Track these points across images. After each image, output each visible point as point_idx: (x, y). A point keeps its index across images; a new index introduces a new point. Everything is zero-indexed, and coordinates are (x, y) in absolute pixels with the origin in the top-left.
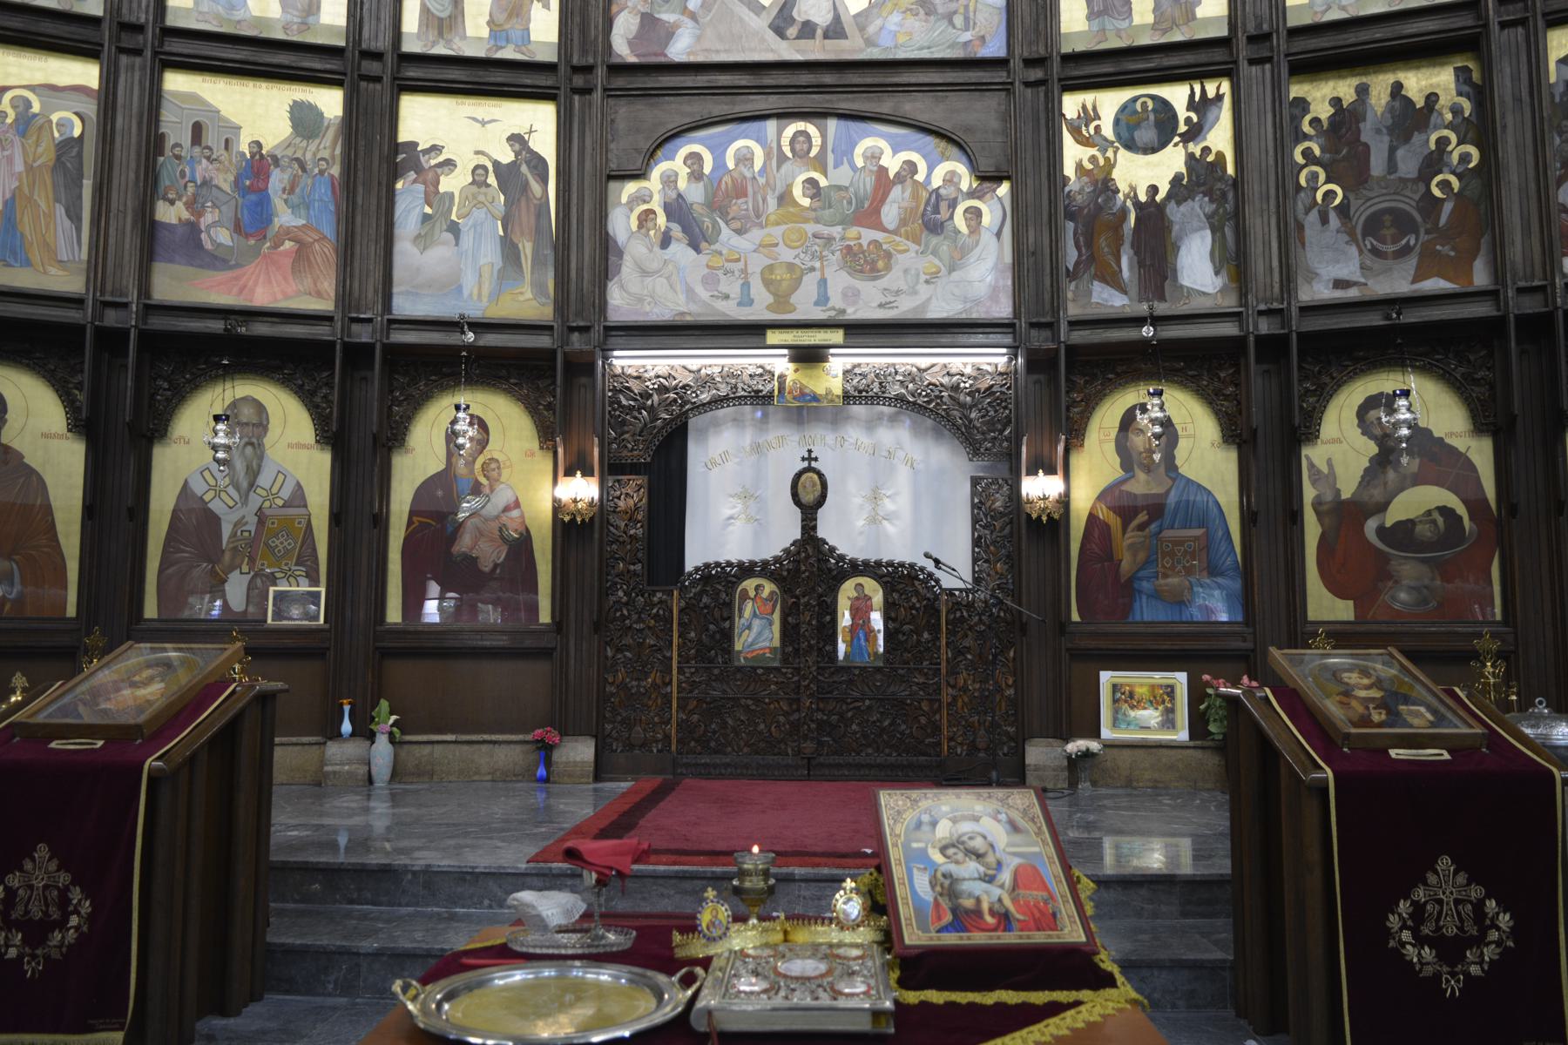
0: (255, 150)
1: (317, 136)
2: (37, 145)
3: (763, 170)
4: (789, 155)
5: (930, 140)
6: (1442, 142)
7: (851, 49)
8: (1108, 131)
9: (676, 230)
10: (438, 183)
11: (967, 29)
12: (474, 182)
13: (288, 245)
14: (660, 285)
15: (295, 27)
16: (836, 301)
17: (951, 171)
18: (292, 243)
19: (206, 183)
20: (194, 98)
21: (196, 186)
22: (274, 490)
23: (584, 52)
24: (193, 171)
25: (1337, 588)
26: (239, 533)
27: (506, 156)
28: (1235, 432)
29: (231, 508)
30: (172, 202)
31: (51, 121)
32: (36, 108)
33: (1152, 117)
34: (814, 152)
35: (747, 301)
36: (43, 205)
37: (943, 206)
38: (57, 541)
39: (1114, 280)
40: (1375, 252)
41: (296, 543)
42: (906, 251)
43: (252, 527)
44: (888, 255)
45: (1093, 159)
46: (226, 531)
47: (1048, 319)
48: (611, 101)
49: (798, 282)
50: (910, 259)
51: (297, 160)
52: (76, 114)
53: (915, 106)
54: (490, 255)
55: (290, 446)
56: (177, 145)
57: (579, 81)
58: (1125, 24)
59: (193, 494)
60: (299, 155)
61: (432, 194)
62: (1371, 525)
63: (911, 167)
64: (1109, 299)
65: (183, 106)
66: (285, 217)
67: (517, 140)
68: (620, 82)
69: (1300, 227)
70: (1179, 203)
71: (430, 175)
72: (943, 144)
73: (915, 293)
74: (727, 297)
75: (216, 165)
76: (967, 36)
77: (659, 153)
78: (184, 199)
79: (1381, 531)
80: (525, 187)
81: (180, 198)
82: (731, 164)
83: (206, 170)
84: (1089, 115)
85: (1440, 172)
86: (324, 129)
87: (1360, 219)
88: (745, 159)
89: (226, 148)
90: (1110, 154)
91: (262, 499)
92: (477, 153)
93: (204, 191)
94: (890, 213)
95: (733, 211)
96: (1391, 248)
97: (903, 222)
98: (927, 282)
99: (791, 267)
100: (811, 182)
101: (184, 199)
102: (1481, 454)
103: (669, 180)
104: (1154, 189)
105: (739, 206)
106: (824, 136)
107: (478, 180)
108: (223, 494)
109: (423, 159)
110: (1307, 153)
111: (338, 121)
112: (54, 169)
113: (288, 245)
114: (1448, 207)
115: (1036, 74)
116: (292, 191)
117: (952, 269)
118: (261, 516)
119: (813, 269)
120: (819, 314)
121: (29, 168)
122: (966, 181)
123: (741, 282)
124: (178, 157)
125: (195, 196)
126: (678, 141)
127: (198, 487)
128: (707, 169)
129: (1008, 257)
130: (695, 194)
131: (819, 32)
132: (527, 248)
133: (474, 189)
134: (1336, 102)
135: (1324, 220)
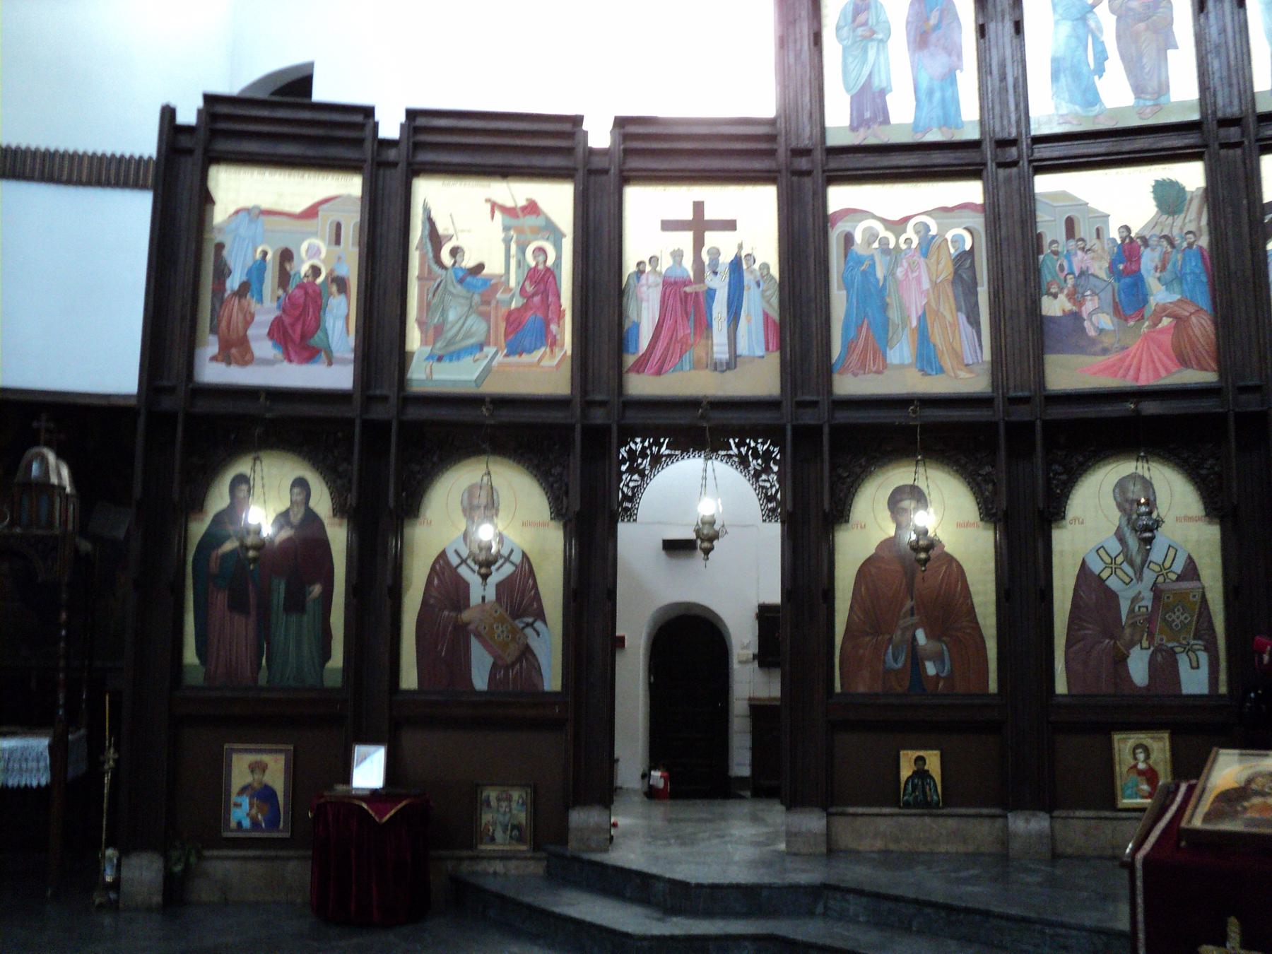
0: (1125, 234)
1: (1180, 212)
2: (938, 263)
13: (1166, 321)
15: (1148, 110)
18: (1170, 320)
19: (1083, 273)
20: (1064, 195)
21: (1075, 277)
22: (1167, 564)
24: (1070, 263)
26: (1137, 608)
29: (1127, 584)
30: (1055, 296)
31: (946, 240)
32: (934, 231)
36: (949, 317)
38: (977, 623)
41: (1192, 616)
43: (1148, 602)
51: (1165, 237)
52: (967, 229)
55: (1178, 519)
59: (1092, 573)
60: (1166, 232)
65: (1055, 204)
66: (1159, 295)
75: (1090, 254)
78: (1066, 291)
81: (1061, 290)
83: (1082, 261)
86: (1187, 202)
89: (1098, 236)
91: (1156, 575)
93: (1082, 281)
101: (1066, 291)
108: (1119, 572)
111: (1201, 192)
112: (953, 283)
113: (1166, 321)
116: (1164, 268)
118: (1155, 588)
121: (935, 285)
124: (1056, 253)
125: (1075, 286)
127: (1096, 566)
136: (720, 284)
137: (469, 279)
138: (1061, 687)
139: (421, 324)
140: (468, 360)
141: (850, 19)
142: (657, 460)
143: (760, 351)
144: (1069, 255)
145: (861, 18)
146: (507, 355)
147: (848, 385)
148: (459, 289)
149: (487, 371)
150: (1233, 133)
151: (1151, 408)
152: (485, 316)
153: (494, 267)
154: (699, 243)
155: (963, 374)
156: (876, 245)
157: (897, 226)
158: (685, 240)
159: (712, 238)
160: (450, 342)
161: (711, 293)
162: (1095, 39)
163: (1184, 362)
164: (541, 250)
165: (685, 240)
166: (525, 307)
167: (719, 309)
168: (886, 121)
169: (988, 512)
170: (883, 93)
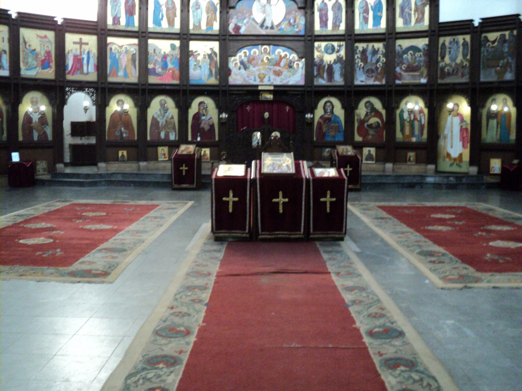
3: (258, 55)
4: (263, 51)
5: (290, 50)
6: (380, 57)
8: (323, 49)
9: (242, 67)
10: (196, 58)
11: (297, 28)
12: (203, 58)
13: (171, 71)
16: (272, 81)
17: (294, 56)
23: (224, 31)
24: (154, 58)
25: (360, 134)
28: (344, 107)
32: (128, 49)
34: (268, 52)
35: (255, 80)
39: (323, 78)
40: (368, 76)
42: (285, 71)
43: (164, 122)
44: (282, 72)
45: (320, 55)
46: (160, 124)
47: (310, 85)
48: (230, 42)
49: (264, 77)
50: (285, 72)
53: (288, 44)
54: (207, 72)
56: (151, 54)
57: (223, 38)
60: (172, 54)
61: (196, 60)
62: (366, 124)
63: (286, 55)
64: (322, 82)
66: (170, 66)
67: (211, 49)
68: (231, 38)
69: (356, 70)
71: (195, 57)
72: (292, 51)
76: (297, 30)
77: (239, 51)
79: (368, 125)
82: (252, 53)
84: (319, 47)
87: (366, 70)
88: (255, 53)
90: (323, 54)
92: (204, 52)
94: (282, 64)
95: (252, 63)
96: (370, 75)
97: (285, 65)
99: (263, 74)
100: (267, 58)
102: (383, 112)
103: (240, 57)
104: (331, 62)
105: (253, 62)
106: (270, 48)
107: (204, 58)
110: (358, 56)
112: (131, 59)
114: (380, 69)
115: (309, 38)
117: (293, 75)
118: (166, 121)
119: (267, 75)
120: (269, 83)
123: (254, 77)
126: (242, 49)
127: (155, 116)
128: (248, 54)
130: (245, 60)
131: (269, 28)
132: (214, 70)
133: (203, 59)
134: (363, 47)
135: (360, 69)
136: (85, 56)
137: (33, 52)
138: (149, 138)
139: (23, 62)
140: (33, 70)
142: (71, 93)
143: (93, 71)
144: (154, 56)
146: (42, 69)
147: (111, 79)
148: (30, 54)
149: (37, 73)
150: (185, 36)
151: (168, 87)
152: (36, 61)
153: (38, 50)
156: (116, 51)
159: (83, 46)
160: (29, 66)
161: (83, 58)
163: (173, 78)
164: (48, 46)
165: (78, 46)
166: (45, 60)
167: (85, 62)
168: (120, 24)
169: (136, 105)
170: (119, 18)
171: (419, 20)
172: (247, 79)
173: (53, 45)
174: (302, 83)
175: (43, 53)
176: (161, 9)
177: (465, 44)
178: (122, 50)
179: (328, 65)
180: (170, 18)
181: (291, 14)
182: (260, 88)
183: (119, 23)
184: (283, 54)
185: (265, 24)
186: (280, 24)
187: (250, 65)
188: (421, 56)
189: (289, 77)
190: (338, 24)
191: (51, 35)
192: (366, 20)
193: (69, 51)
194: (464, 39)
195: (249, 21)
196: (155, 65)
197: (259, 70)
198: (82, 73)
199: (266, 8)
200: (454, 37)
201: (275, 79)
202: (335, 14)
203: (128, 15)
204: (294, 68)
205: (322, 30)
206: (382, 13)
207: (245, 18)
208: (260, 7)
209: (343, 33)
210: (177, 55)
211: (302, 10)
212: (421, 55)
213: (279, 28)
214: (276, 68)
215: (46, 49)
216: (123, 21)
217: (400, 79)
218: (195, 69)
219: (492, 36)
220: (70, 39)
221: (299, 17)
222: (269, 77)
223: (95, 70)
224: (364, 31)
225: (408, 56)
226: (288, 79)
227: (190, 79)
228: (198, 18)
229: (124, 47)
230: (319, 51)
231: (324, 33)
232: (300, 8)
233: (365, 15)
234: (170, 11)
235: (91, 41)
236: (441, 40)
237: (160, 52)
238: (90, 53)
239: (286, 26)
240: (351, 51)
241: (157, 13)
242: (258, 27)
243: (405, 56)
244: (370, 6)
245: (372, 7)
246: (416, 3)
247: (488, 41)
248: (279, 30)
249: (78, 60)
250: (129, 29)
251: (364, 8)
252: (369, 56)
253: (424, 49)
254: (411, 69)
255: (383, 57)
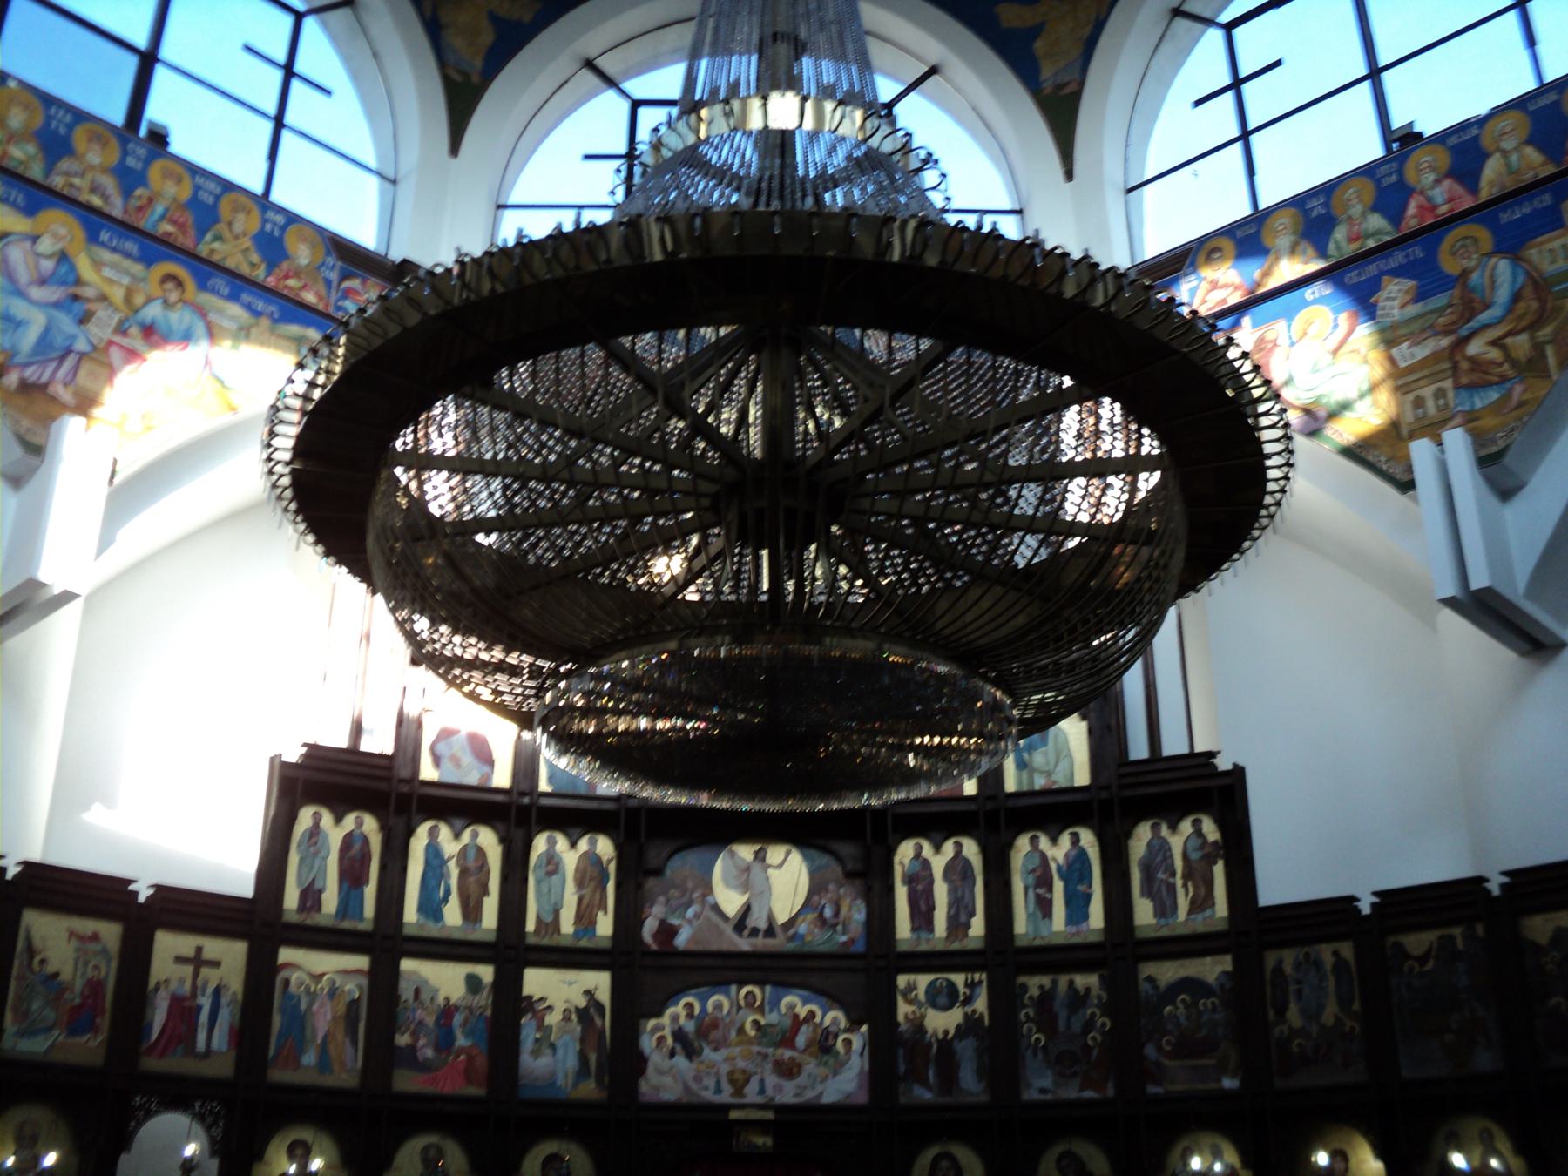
3: (729, 1013)
4: (742, 1003)
5: (824, 1000)
7: (778, 943)
8: (922, 997)
9: (679, 1048)
10: (543, 1019)
11: (844, 933)
12: (563, 1019)
13: (462, 1057)
14: (668, 1080)
17: (834, 1017)
20: (415, 973)
27: (582, 1003)
32: (337, 985)
33: (945, 991)
34: (758, 1003)
35: (718, 1091)
37: (831, 1037)
39: (924, 1082)
42: (809, 1063)
44: (799, 1066)
45: (914, 1012)
49: (747, 1081)
50: (811, 1066)
54: (572, 1062)
56: (405, 1001)
58: (931, 936)
61: (541, 1026)
63: (812, 1015)
64: (923, 1094)
66: (461, 1041)
67: (588, 993)
70: (961, 1040)
71: (540, 1015)
73: (813, 1087)
74: (707, 1088)
76: (844, 938)
77: (671, 1000)
80: (592, 1020)
82: (710, 1008)
84: (912, 987)
85: (1090, 1032)
88: (719, 1006)
90: (923, 1009)
94: (801, 1041)
97: (808, 1046)
98: (822, 1082)
99: (744, 1071)
100: (756, 1022)
103: (675, 1018)
104: (946, 1032)
105: (714, 1035)
106: (763, 992)
109: (536, 1005)
114: (1095, 1052)
117: (835, 1073)
119: (756, 1073)
120: (759, 1100)
122: (843, 1024)
123: (715, 1080)
129: (867, 1067)
130: (690, 1027)
131: (761, 934)
132: (593, 1057)
133: (563, 1023)
134: (1041, 987)
135: (1035, 1055)
136: (205, 1002)
139: (15, 1010)
141: (307, 838)
142: (149, 1115)
143: (224, 1047)
144: (414, 1010)
145: (313, 840)
147: (278, 1075)
153: (66, 974)
154: (196, 974)
155: (344, 1076)
156: (302, 989)
157: (318, 978)
158: (188, 970)
159: (205, 971)
161: (199, 1008)
162: (446, 883)
165: (188, 970)
168: (319, 909)
170: (320, 892)
171: (1202, 902)
172: (694, 1086)
173: (114, 965)
174: (862, 1098)
175: (79, 984)
176: (445, 871)
177: (1340, 965)
178: (319, 986)
179: (938, 1040)
180: (468, 897)
181: (827, 891)
182: (734, 1115)
183: (317, 905)
184: (802, 1011)
185: (752, 922)
186: (792, 922)
187: (704, 1045)
188: (1214, 1010)
189: (824, 1079)
190: (963, 918)
191: (111, 932)
192: (1045, 906)
193: (158, 983)
194: (1336, 953)
195: (702, 913)
196: (415, 1035)
197: (728, 1059)
198: (191, 1050)
199: (751, 876)
200: (1306, 949)
201: (778, 1088)
202: (952, 891)
203: (346, 886)
204: (838, 1053)
205: (919, 938)
206: (1090, 886)
207: (689, 904)
208: (734, 872)
209: (978, 945)
210: (485, 1009)
211: (858, 882)
212: (1213, 1003)
213: (792, 932)
214: (783, 1054)
215: (90, 973)
216: (330, 901)
217: (1158, 1083)
218: (536, 1053)
219: (1418, 942)
220: (169, 946)
221: (848, 901)
222: (762, 1082)
223: (229, 1045)
224: (1042, 938)
225: (1177, 1008)
226: (819, 1088)
227: (521, 1082)
228: (552, 902)
229: (326, 977)
230: (910, 1002)
231: (924, 947)
232: (850, 875)
233: (1041, 891)
234: (472, 879)
235: (230, 955)
236: (1271, 959)
237: (432, 999)
238: (223, 992)
239: (812, 927)
240: (1004, 999)
241: (433, 883)
242: (728, 930)
243: (1168, 1008)
244: (1053, 866)
245: (1059, 869)
246: (1185, 856)
247: (1408, 956)
248: (793, 938)
249: (184, 1011)
250: (347, 925)
251: (1038, 873)
252: (1062, 1015)
253: (1222, 986)
254: (1187, 1047)
255: (1102, 1016)
